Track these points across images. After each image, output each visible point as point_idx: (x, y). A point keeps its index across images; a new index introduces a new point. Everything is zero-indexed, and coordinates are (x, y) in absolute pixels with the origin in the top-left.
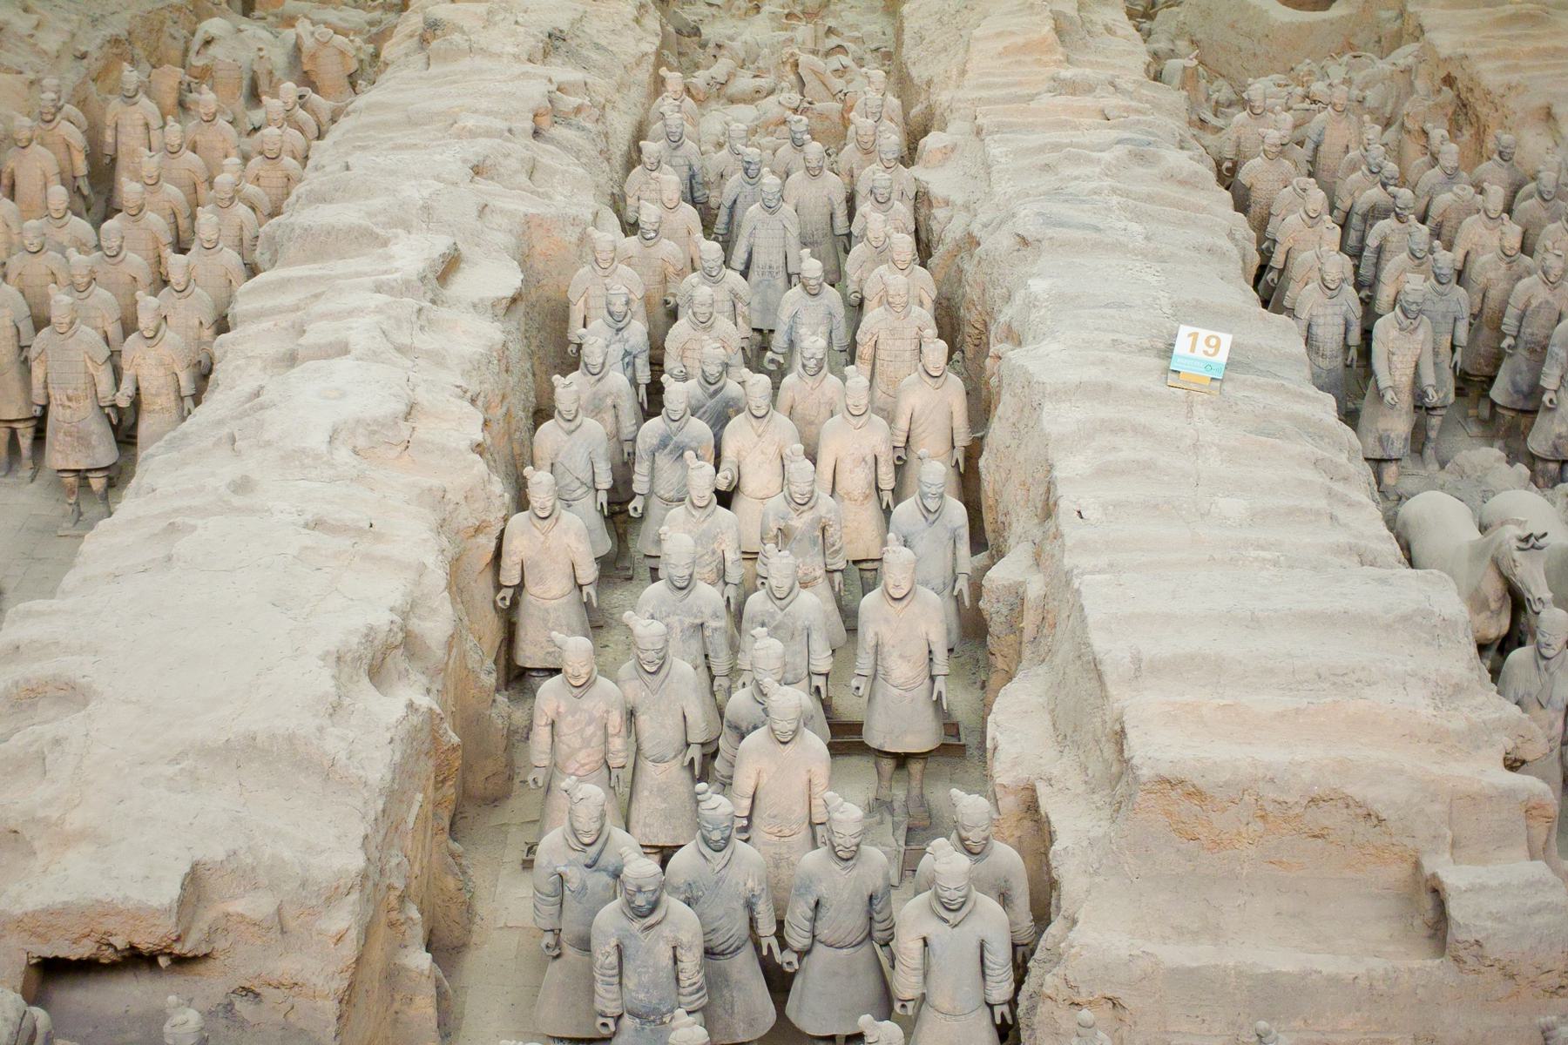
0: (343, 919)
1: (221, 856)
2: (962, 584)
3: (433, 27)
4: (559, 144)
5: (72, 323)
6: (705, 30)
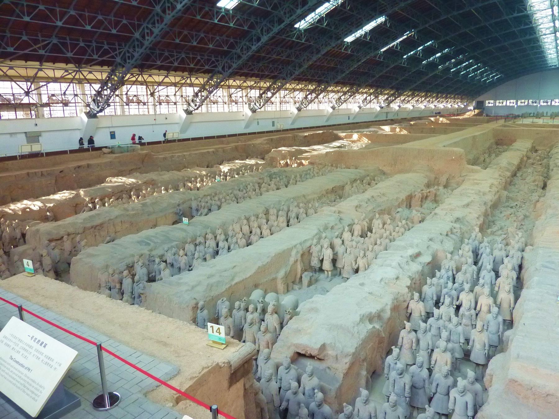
0: (348, 360)
1: (329, 343)
2: (500, 333)
3: (435, 214)
4: (451, 238)
5: (350, 253)
6: (495, 222)
